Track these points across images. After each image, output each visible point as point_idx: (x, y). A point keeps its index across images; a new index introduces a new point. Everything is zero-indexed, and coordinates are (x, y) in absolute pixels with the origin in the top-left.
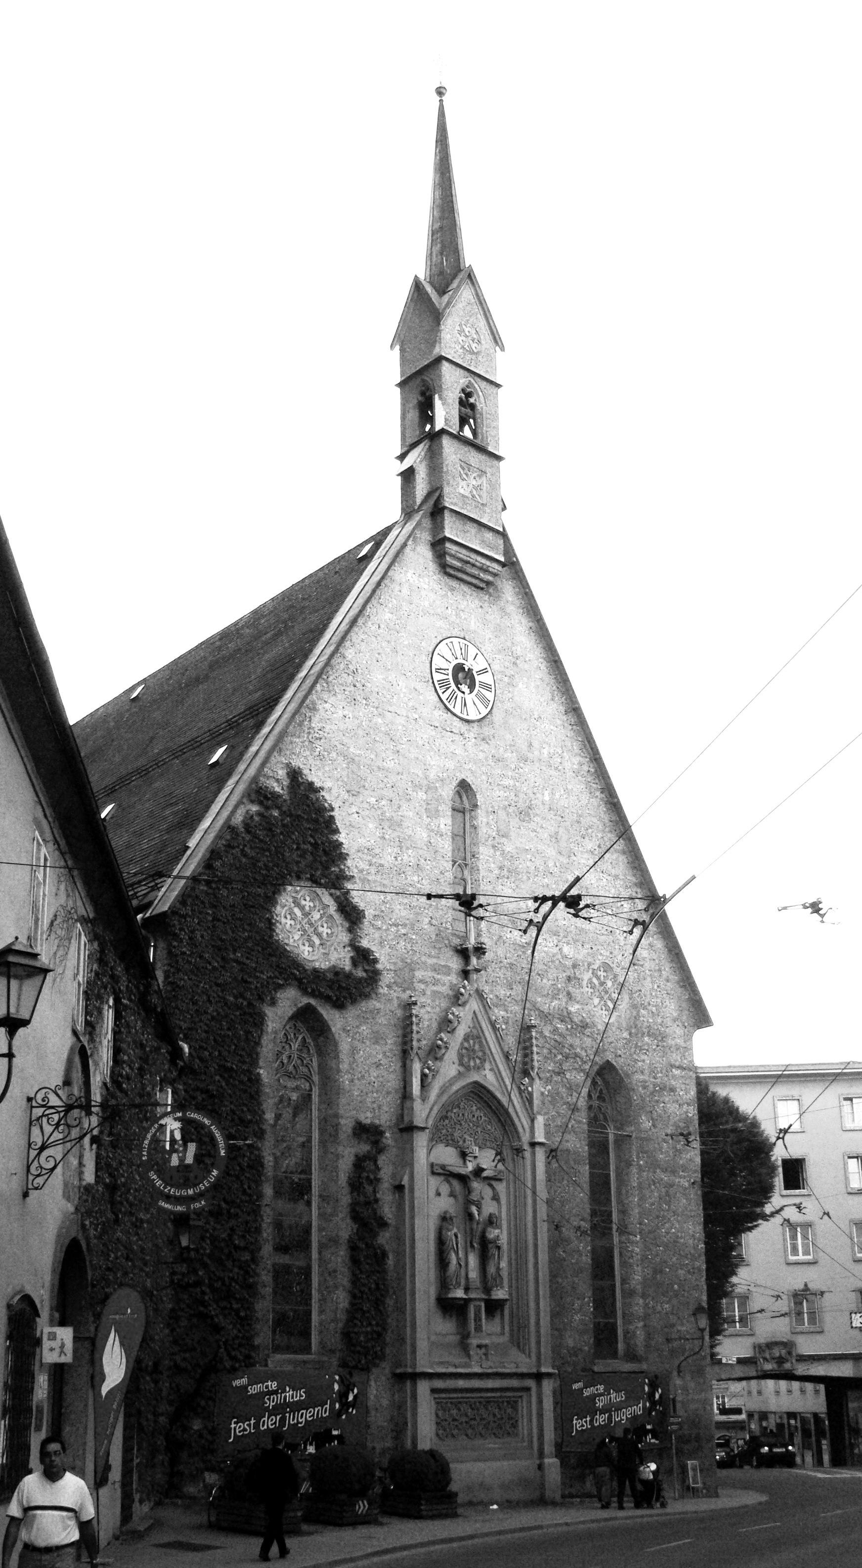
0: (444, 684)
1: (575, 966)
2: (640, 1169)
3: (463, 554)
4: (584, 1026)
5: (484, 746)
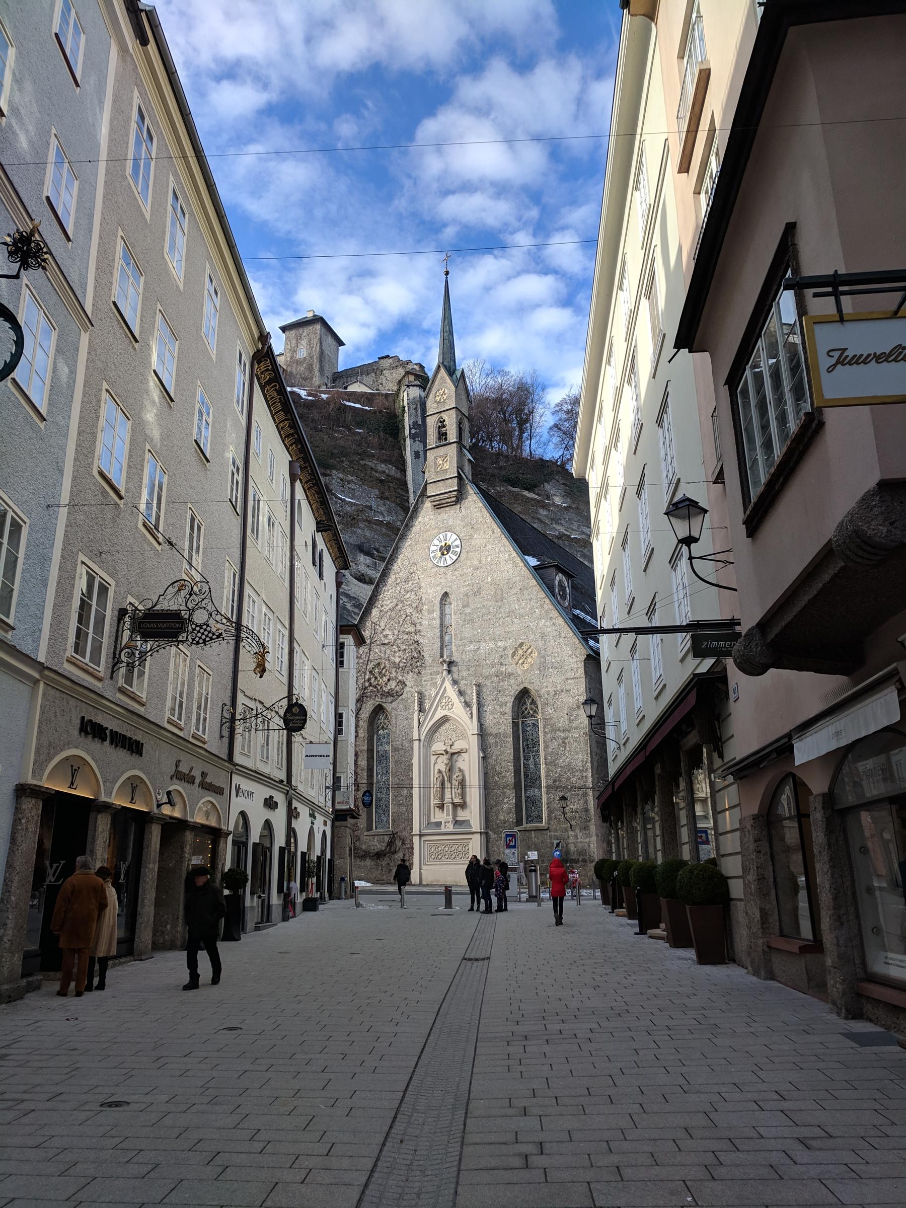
0: (434, 557)
2: (545, 733)
3: (437, 498)
4: (510, 675)
5: (456, 573)
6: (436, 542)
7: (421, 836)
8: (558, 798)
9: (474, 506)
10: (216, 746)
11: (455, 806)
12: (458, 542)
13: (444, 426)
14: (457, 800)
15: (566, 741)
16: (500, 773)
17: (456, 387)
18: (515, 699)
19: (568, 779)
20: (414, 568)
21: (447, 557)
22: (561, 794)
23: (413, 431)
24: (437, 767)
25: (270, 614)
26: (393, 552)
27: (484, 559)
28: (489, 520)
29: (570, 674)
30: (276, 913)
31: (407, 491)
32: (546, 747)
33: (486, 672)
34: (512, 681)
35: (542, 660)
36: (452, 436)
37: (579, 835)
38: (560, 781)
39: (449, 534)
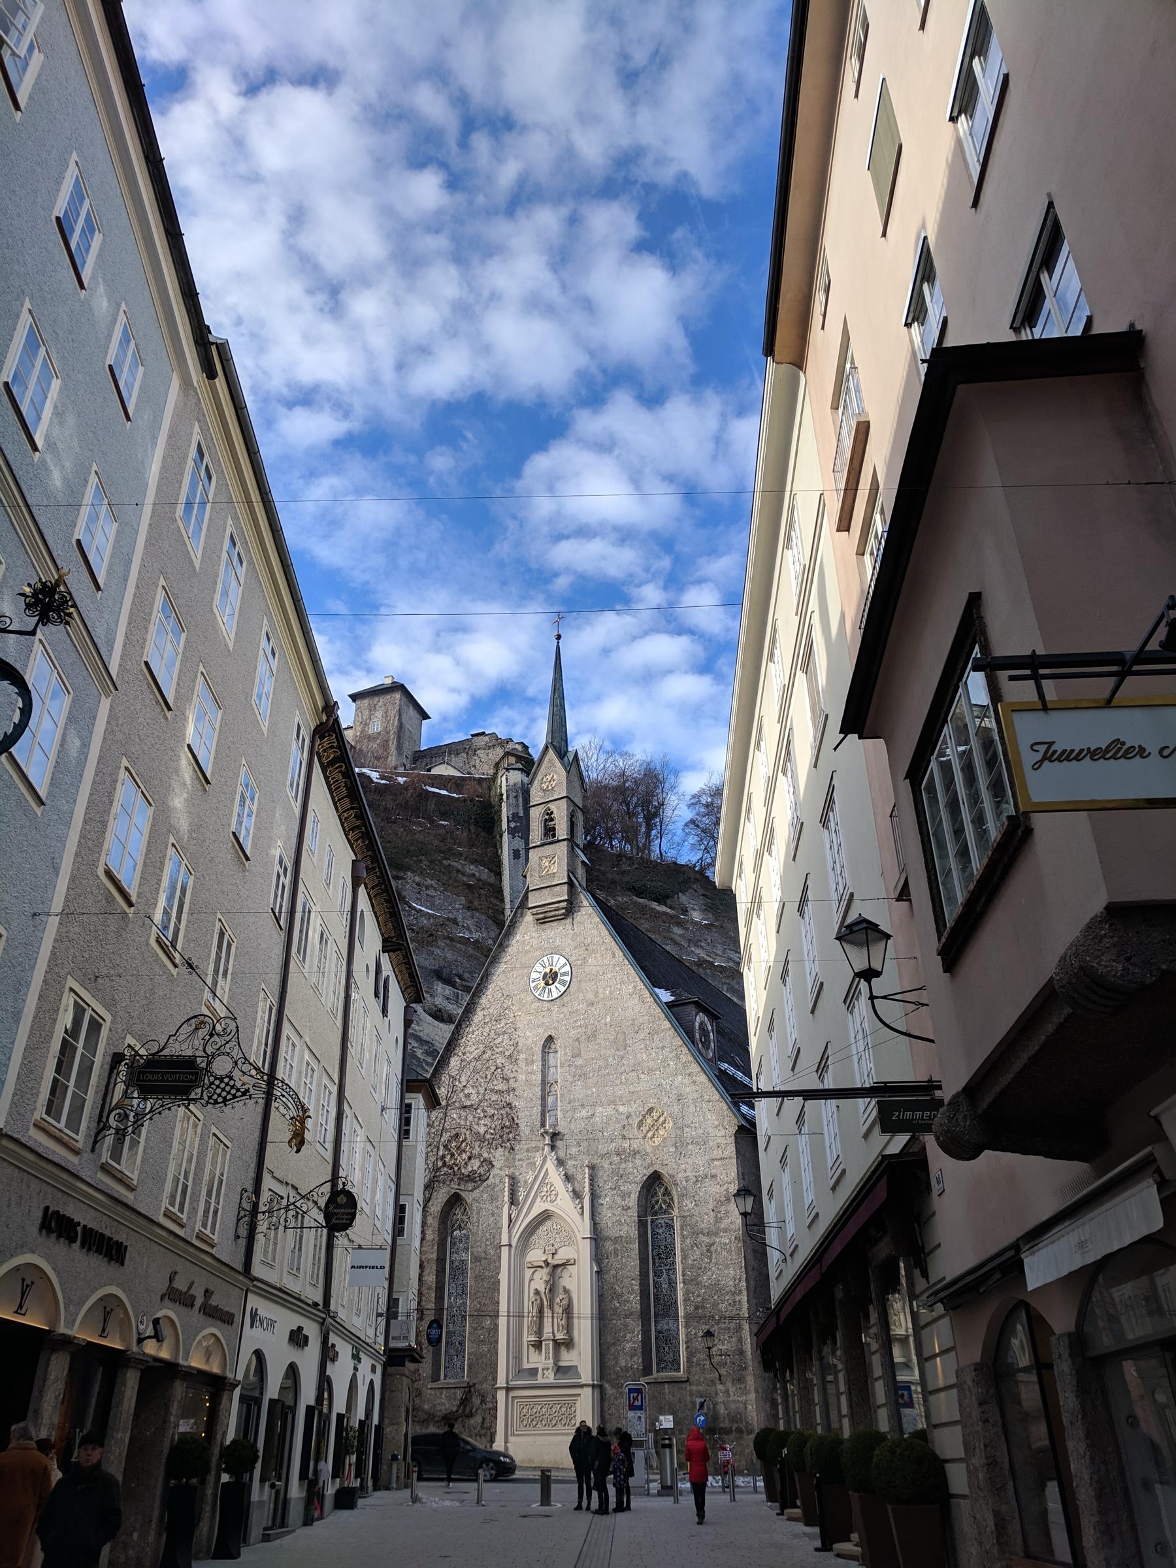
0: (536, 988)
1: (628, 1117)
4: (635, 1153)
5: (565, 1009)
6: (538, 967)
7: (508, 1389)
8: (701, 1334)
9: (589, 921)
10: (227, 1250)
11: (557, 1344)
12: (567, 968)
13: (552, 820)
14: (560, 1336)
15: (712, 1249)
16: (621, 1295)
17: (568, 772)
18: (642, 1188)
19: (715, 1305)
20: (508, 1003)
21: (553, 987)
22: (705, 1328)
23: (512, 825)
24: (534, 1286)
25: (314, 1063)
26: (482, 980)
27: (601, 991)
28: (609, 939)
29: (717, 1153)
30: (296, 1511)
31: (502, 900)
32: (685, 1257)
33: (603, 1148)
34: (638, 1162)
35: (679, 1132)
36: (562, 831)
37: (732, 1390)
38: (703, 1307)
39: (556, 957)
